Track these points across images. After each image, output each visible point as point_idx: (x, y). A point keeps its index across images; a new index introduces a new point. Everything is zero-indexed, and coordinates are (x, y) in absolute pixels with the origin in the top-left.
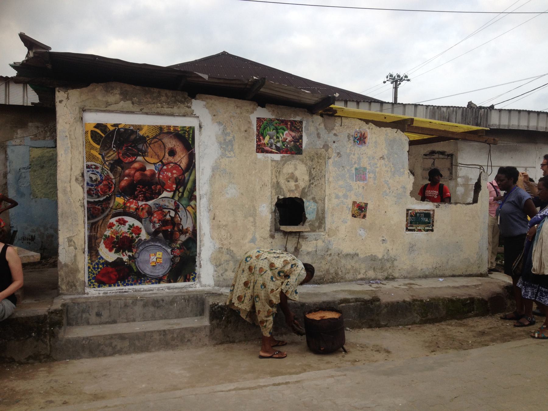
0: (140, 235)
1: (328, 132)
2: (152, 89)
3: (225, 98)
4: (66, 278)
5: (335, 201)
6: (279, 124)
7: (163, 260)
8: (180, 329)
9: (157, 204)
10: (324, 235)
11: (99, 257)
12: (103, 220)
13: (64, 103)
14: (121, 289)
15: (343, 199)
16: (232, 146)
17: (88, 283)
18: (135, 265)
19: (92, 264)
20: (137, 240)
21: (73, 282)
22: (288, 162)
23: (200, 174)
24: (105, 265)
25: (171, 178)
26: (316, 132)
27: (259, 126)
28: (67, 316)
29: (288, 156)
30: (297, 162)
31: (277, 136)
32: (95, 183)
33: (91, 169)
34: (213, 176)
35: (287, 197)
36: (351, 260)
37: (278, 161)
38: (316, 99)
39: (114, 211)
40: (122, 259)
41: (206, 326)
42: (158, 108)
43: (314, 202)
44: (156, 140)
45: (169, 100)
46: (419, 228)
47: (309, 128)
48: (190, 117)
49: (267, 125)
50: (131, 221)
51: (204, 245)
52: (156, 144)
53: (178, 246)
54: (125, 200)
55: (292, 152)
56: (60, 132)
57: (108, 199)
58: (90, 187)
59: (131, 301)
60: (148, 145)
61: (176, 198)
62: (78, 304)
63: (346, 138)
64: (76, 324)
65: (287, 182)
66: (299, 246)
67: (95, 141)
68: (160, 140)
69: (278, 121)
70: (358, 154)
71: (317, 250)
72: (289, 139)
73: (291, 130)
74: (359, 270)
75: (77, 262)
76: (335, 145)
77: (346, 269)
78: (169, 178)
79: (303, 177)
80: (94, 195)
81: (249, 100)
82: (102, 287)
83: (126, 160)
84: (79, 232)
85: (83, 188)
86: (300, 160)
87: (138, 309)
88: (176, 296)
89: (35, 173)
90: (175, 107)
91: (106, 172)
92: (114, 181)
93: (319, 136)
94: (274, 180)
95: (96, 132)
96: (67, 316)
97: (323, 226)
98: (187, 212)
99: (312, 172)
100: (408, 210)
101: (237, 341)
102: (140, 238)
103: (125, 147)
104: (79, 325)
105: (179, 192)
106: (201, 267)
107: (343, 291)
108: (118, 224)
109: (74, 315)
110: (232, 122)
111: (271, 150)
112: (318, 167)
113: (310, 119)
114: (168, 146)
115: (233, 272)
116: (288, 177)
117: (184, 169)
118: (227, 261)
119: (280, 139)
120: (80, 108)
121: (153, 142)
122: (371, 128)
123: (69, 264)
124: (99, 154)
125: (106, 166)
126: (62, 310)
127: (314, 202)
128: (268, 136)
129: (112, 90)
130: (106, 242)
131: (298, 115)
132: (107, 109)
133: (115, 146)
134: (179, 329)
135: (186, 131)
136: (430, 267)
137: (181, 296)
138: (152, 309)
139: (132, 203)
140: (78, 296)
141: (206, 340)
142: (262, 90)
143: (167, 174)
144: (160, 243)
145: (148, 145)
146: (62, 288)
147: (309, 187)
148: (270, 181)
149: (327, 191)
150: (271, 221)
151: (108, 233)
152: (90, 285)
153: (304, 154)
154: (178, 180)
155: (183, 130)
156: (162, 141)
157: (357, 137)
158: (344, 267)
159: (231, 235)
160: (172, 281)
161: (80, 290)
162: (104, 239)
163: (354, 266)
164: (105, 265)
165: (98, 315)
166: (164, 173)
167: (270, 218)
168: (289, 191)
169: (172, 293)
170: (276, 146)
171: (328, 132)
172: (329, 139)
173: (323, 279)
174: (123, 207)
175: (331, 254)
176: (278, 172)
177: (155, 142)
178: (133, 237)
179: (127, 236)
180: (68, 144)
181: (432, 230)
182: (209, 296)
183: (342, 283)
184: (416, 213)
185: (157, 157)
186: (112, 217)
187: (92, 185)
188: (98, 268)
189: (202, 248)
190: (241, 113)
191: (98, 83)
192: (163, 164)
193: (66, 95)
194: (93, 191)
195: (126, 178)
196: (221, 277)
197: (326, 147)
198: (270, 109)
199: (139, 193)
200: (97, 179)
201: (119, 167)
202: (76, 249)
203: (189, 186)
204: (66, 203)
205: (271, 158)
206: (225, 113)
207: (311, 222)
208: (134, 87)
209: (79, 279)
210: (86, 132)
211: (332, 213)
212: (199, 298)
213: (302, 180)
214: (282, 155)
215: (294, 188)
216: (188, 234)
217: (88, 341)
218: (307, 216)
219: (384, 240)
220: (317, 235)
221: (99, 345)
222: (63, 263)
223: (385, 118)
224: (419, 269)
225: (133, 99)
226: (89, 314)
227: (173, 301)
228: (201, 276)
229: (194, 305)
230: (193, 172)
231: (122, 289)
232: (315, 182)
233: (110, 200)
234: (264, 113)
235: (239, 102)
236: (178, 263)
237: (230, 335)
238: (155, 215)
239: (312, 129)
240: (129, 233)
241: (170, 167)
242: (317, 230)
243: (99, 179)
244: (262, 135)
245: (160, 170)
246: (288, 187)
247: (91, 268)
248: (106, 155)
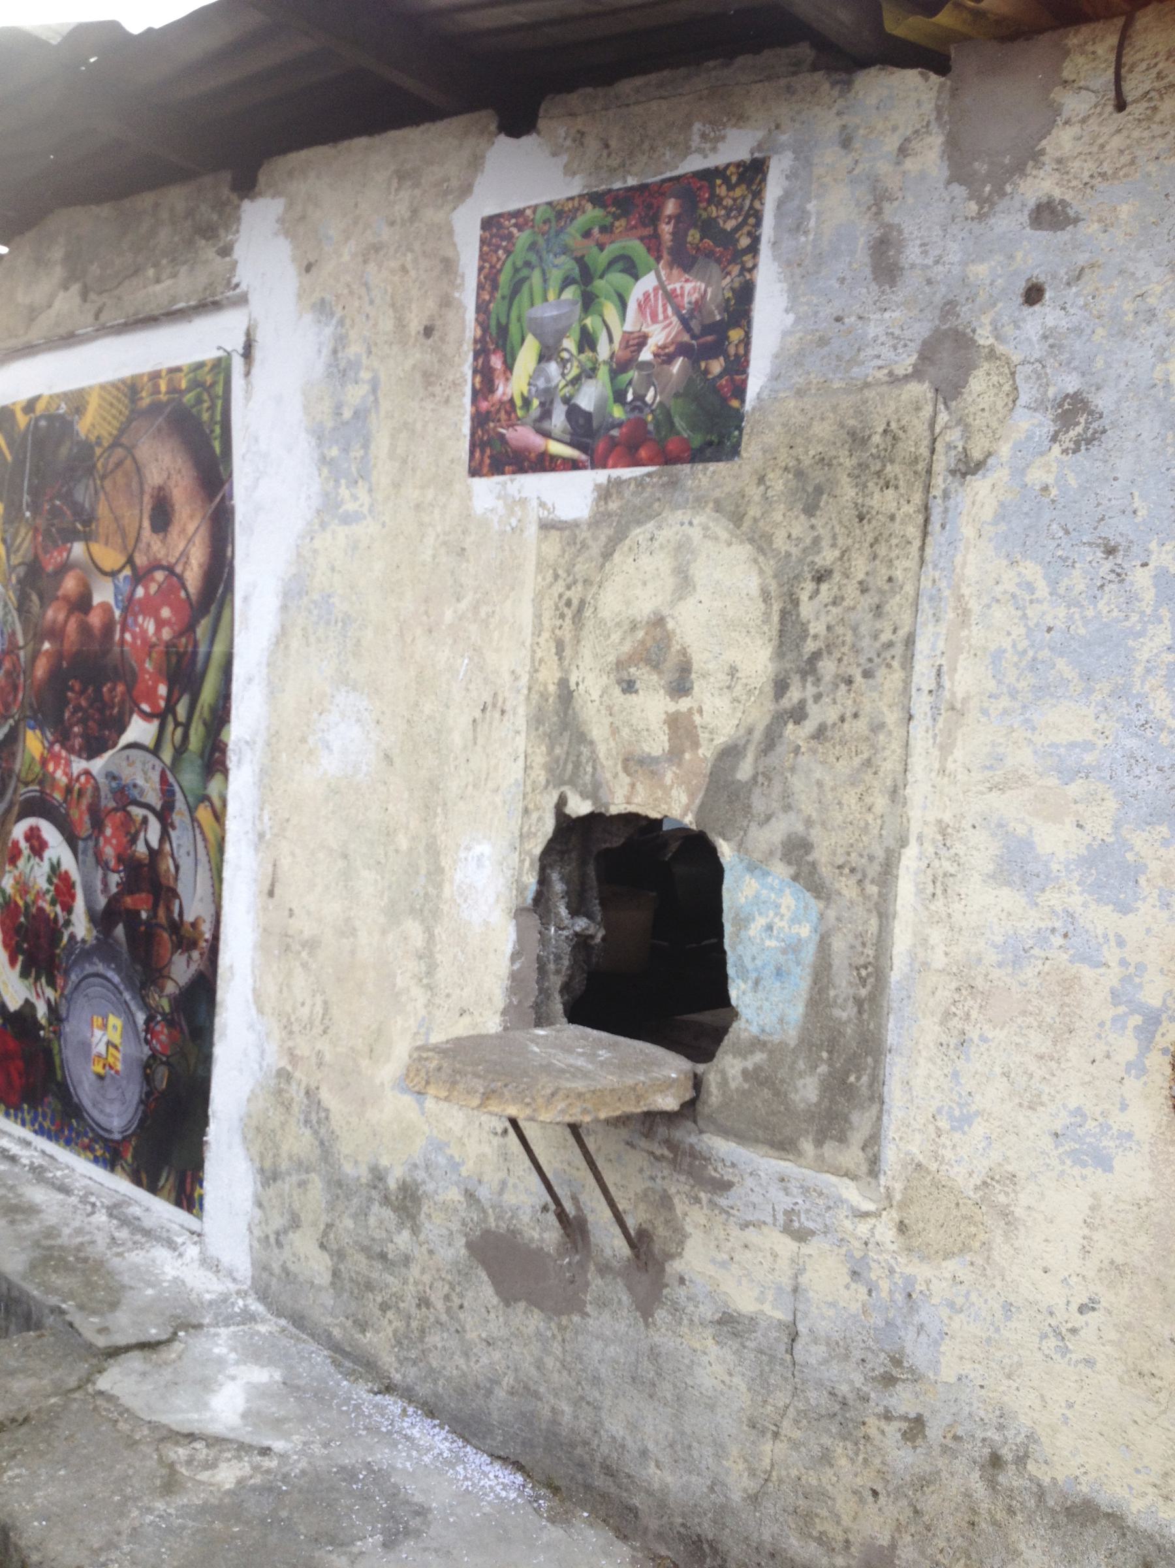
1: (981, 202)
6: (604, 229)
10: (866, 1215)
15: (1076, 901)
22: (639, 534)
26: (864, 232)
27: (489, 280)
29: (640, 483)
31: (584, 331)
34: (282, 637)
35: (614, 810)
37: (575, 524)
43: (795, 878)
47: (811, 207)
49: (533, 258)
53: (165, 1004)
55: (672, 446)
65: (617, 691)
71: (802, 1328)
72: (659, 336)
73: (684, 261)
79: (732, 655)
86: (718, 507)
94: (543, 675)
97: (855, 1117)
99: (806, 609)
105: (177, 724)
110: (368, 289)
111: (537, 441)
112: (860, 566)
116: (627, 648)
117: (194, 598)
121: (111, 466)
127: (795, 878)
131: (741, 119)
144: (118, 970)
147: (771, 740)
148: (524, 680)
149: (917, 791)
150: (514, 976)
153: (751, 449)
154: (174, 660)
167: (508, 947)
170: (573, 412)
171: (973, 207)
176: (569, 613)
190: (415, 212)
192: (140, 577)
196: (276, 1251)
198: (562, 132)
203: (207, 694)
205: (542, 505)
207: (759, 1057)
211: (948, 1015)
213: (723, 678)
214: (601, 476)
215: (657, 744)
216: (195, 955)
218: (733, 993)
220: (805, 1191)
232: (818, 698)
236: (162, 1093)
238: (108, 832)
242: (807, 1146)
246: (625, 732)
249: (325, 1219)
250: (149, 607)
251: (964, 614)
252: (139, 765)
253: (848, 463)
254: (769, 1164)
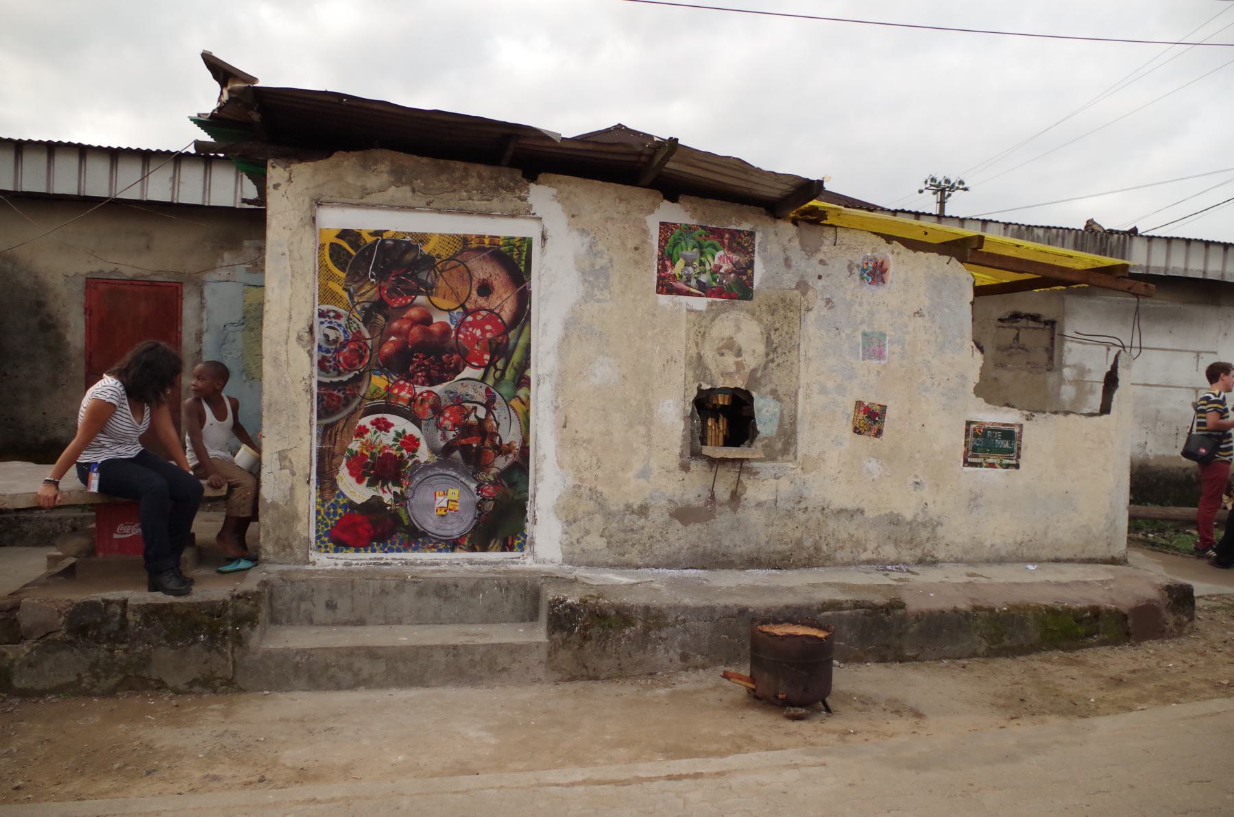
0: (417, 454)
2: (452, 163)
3: (596, 181)
4: (274, 530)
5: (818, 399)
6: (706, 236)
7: (461, 505)
8: (488, 645)
9: (452, 393)
11: (337, 492)
12: (347, 420)
13: (282, 189)
14: (378, 559)
16: (607, 278)
17: (316, 542)
18: (407, 512)
19: (323, 506)
20: (410, 463)
21: (287, 539)
23: (540, 334)
24: (348, 510)
25: (481, 340)
27: (663, 240)
28: (271, 606)
29: (722, 303)
30: (742, 315)
31: (701, 261)
32: (334, 347)
33: (327, 319)
34: (566, 338)
36: (847, 522)
37: (701, 311)
38: (785, 187)
39: (368, 404)
40: (381, 498)
41: (540, 643)
42: (461, 200)
44: (454, 263)
45: (484, 185)
46: (990, 461)
47: (768, 246)
48: (523, 218)
50: (400, 424)
51: (542, 479)
52: (454, 272)
53: (492, 479)
54: (389, 382)
57: (358, 379)
58: (324, 354)
59: (393, 584)
60: (438, 273)
61: (490, 381)
62: (293, 582)
63: (846, 269)
64: (287, 621)
66: (739, 489)
67: (337, 263)
68: (463, 263)
69: (703, 231)
70: (869, 304)
72: (726, 267)
74: (863, 542)
75: (295, 501)
76: (821, 282)
77: (838, 540)
78: (477, 341)
80: (331, 370)
81: (644, 187)
82: (341, 551)
83: (395, 302)
84: (299, 442)
85: (311, 356)
86: (747, 311)
87: (407, 599)
88: (482, 579)
89: (252, 333)
90: (495, 200)
91: (355, 325)
92: (369, 343)
93: (787, 263)
95: (340, 246)
96: (271, 606)
97: (791, 449)
98: (511, 410)
99: (773, 337)
100: (969, 423)
101: (603, 676)
102: (416, 458)
103: (393, 277)
104: (293, 625)
105: (497, 370)
106: (535, 523)
107: (829, 584)
108: (375, 429)
109: (284, 604)
111: (686, 288)
112: (786, 328)
113: (771, 230)
114: (477, 276)
115: (601, 536)
116: (721, 344)
118: (589, 513)
119: (708, 267)
120: (312, 200)
121: (448, 267)
122: (896, 251)
123: (280, 503)
124: (345, 289)
125: (355, 314)
126: (258, 593)
128: (681, 260)
129: (375, 165)
130: (350, 464)
131: (747, 221)
132: (361, 201)
133: (374, 274)
134: (485, 645)
135: (514, 245)
136: (1011, 541)
137: (493, 579)
138: (434, 602)
139: (402, 388)
140: (293, 567)
141: (540, 672)
142: (670, 165)
143: (474, 331)
144: (456, 469)
145: (438, 273)
146: (265, 550)
147: (765, 367)
150: (684, 436)
151: (355, 445)
152: (320, 547)
153: (756, 299)
154: (494, 345)
155: (509, 244)
156: (466, 267)
157: (867, 269)
158: (834, 535)
159: (598, 460)
160: (478, 548)
161: (299, 555)
162: (348, 457)
163: (853, 535)
164: (348, 510)
165: (331, 606)
166: (467, 330)
167: (682, 428)
168: (722, 375)
169: (477, 571)
170: (698, 282)
171: (806, 257)
172: (809, 270)
173: (789, 558)
174: (386, 395)
175: (806, 508)
177: (452, 268)
178: (402, 456)
179: (391, 454)
180: (285, 268)
181: (1017, 466)
182: (549, 584)
183: (827, 569)
184: (986, 430)
185: (454, 297)
186: (365, 415)
187: (328, 351)
188: (335, 514)
189: (539, 485)
190: (628, 212)
191: (348, 151)
192: (467, 312)
193: (287, 175)
194: (330, 362)
195: (393, 338)
197: (803, 286)
199: (417, 368)
200: (337, 338)
201: (380, 317)
202: (293, 474)
203: (516, 357)
204: (278, 383)
205: (687, 304)
206: (595, 212)
207: (766, 441)
208: (419, 158)
209: (298, 533)
210: (322, 247)
212: (529, 585)
214: (710, 299)
215: (733, 369)
216: (511, 456)
217: (306, 657)
218: (758, 428)
219: (917, 483)
221: (327, 666)
222: (269, 501)
223: (926, 234)
224: (988, 543)
225: (415, 182)
226: (314, 605)
227: (476, 587)
228: (537, 541)
229: (519, 599)
230: (526, 329)
231: (381, 559)
233: (361, 380)
234: (676, 213)
235: (626, 190)
236: (490, 512)
237: (588, 665)
238: (447, 415)
239: (774, 248)
240: (395, 448)
241: (479, 318)
242: (780, 458)
243: (342, 339)
244: (670, 257)
245: (461, 324)
246: (721, 367)
247: (322, 513)
249: (603, 527)
250: (474, 324)
251: (810, 340)
252: (471, 387)
253: (782, 305)
254: (769, 465)
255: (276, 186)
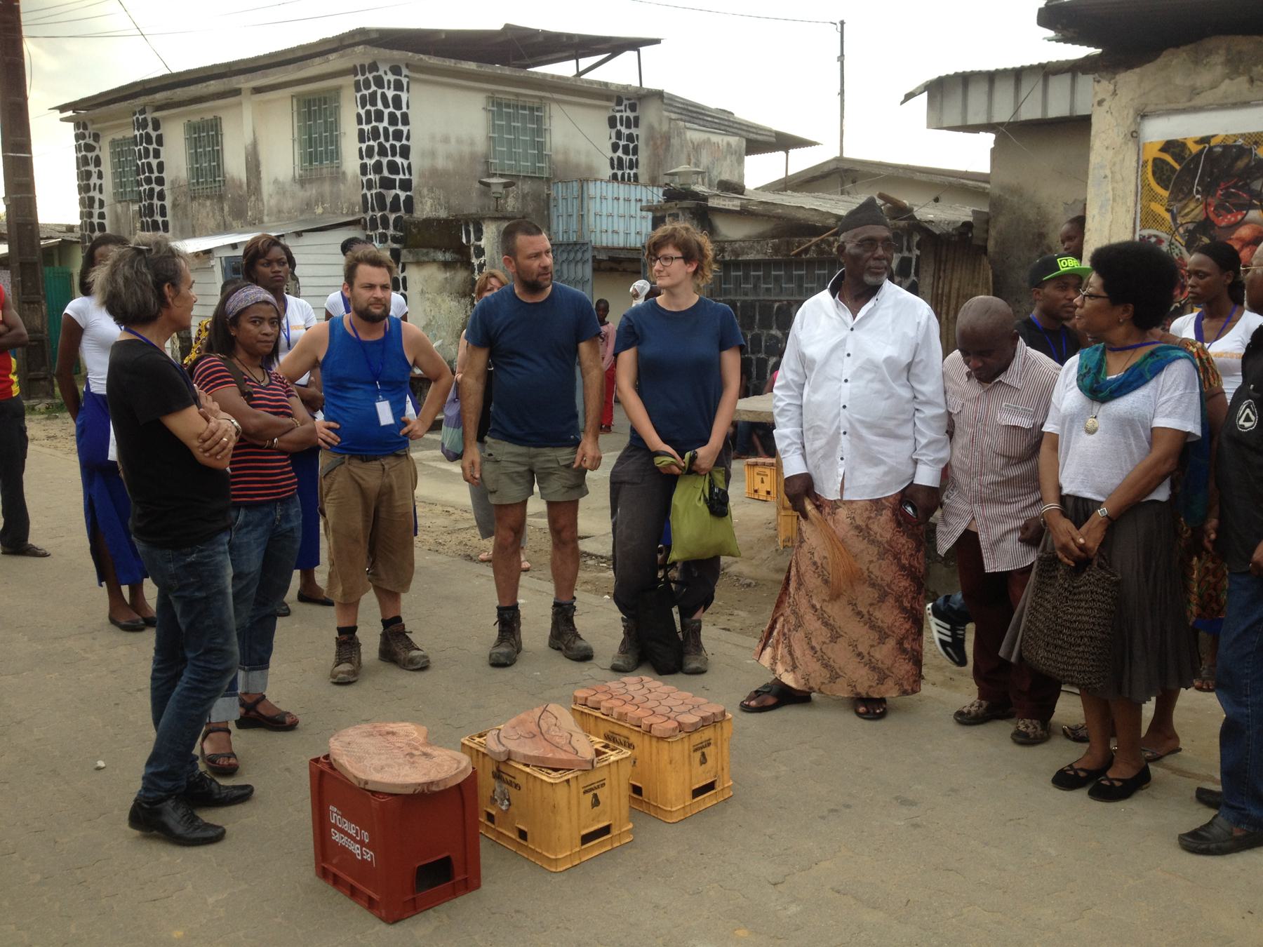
13: (1106, 104)
56: (1094, 169)
124: (1168, 210)
125: (1178, 238)
180: (1107, 192)
193: (1112, 87)
248: (1180, 212)
255: (1100, 103)
